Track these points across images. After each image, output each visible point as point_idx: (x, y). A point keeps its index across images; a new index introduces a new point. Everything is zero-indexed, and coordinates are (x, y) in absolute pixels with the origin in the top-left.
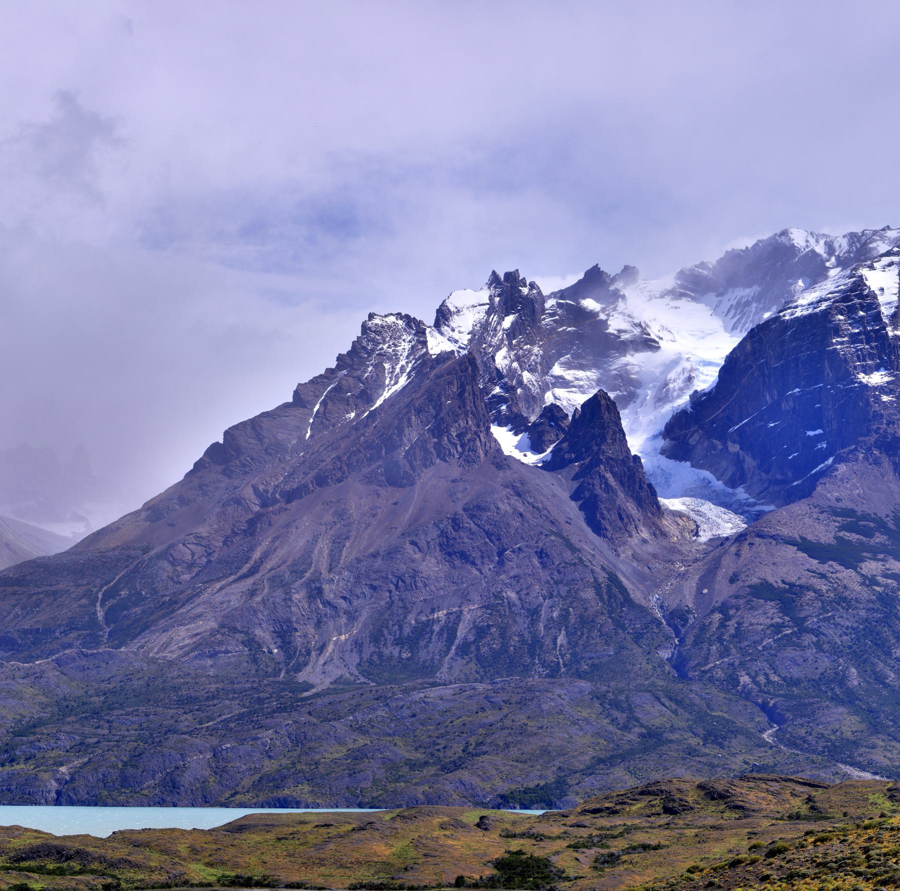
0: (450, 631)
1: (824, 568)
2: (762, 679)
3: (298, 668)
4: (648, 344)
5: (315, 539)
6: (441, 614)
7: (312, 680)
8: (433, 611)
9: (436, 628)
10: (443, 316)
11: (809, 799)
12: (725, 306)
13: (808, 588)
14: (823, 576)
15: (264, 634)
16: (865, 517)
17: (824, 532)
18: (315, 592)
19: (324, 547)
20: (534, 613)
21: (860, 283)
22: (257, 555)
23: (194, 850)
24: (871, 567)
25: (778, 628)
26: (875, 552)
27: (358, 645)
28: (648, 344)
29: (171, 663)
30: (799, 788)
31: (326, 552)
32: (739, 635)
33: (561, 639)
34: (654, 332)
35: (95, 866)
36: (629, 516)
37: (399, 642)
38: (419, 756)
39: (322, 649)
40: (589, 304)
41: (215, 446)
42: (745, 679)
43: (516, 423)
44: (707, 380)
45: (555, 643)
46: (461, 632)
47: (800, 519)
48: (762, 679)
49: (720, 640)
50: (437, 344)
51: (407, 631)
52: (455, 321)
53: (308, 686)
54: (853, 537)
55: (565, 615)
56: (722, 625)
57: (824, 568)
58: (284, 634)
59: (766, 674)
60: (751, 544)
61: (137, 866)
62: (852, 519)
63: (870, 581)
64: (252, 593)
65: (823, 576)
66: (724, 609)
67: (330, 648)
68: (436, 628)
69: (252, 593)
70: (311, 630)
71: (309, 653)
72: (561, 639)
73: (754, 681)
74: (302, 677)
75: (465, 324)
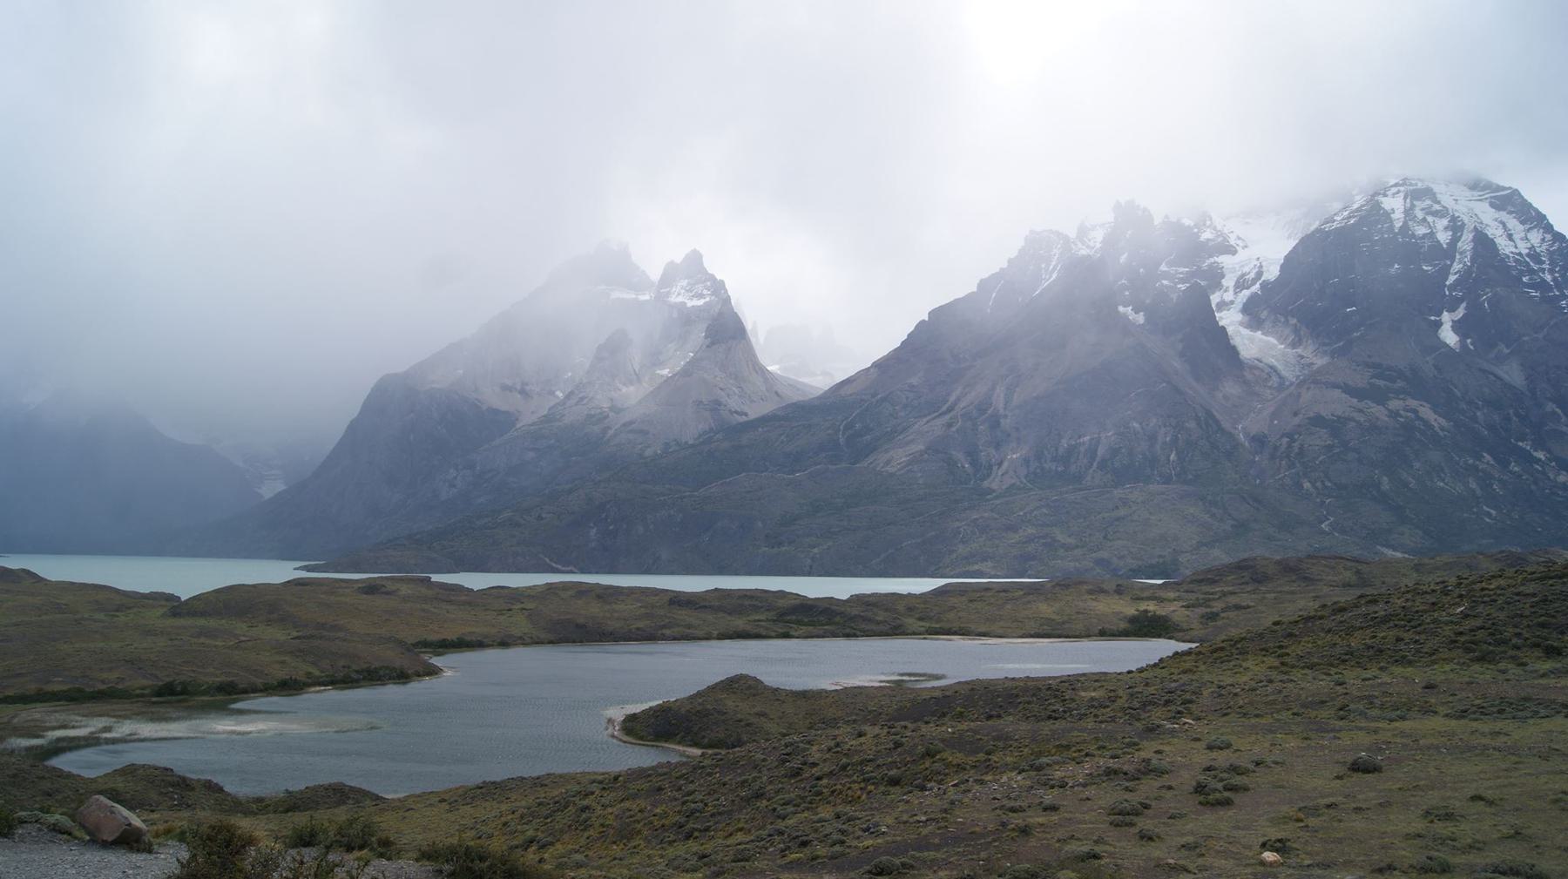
0: (1092, 453)
1: (1361, 405)
3: (983, 480)
7: (994, 486)
9: (1082, 449)
11: (1358, 572)
13: (1352, 419)
14: (1361, 411)
15: (959, 456)
18: (995, 423)
20: (1152, 438)
21: (1378, 205)
22: (952, 399)
23: (910, 609)
24: (1395, 404)
25: (1330, 448)
27: (1026, 461)
29: (892, 475)
30: (1349, 564)
33: (1172, 457)
35: (838, 619)
37: (1054, 459)
38: (1071, 541)
39: (1000, 464)
41: (922, 322)
42: (1307, 485)
46: (1101, 452)
49: (1288, 457)
51: (1061, 451)
54: (1381, 383)
55: (1175, 440)
56: (1289, 446)
57: (1361, 405)
58: (972, 454)
61: (870, 620)
63: (1394, 414)
64: (950, 425)
65: (1361, 411)
66: (1290, 435)
67: (1006, 464)
68: (1082, 449)
69: (950, 425)
70: (992, 451)
71: (990, 467)
72: (1172, 457)
73: (1313, 485)
74: (986, 484)
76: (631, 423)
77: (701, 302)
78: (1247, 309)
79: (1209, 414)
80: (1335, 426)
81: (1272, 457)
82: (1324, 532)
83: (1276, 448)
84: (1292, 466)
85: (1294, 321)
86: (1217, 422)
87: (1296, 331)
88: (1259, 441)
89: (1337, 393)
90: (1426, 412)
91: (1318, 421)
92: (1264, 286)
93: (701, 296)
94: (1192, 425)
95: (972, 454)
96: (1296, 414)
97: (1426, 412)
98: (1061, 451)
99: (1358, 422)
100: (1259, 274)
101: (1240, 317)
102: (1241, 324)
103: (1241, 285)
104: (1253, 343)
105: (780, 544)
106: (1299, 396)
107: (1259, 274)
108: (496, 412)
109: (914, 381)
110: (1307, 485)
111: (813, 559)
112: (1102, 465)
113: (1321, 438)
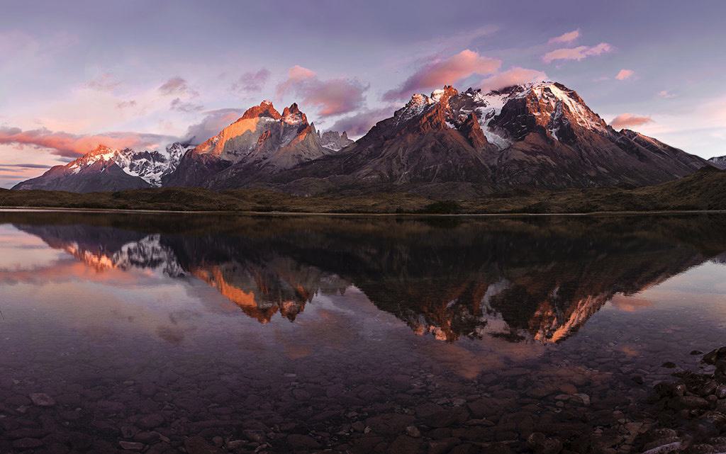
0: (434, 171)
4: (485, 105)
6: (432, 167)
16: (537, 145)
17: (528, 148)
24: (539, 157)
26: (540, 153)
28: (485, 105)
33: (464, 173)
34: (485, 102)
39: (400, 176)
40: (469, 95)
42: (511, 183)
44: (498, 113)
47: (521, 145)
50: (431, 101)
62: (534, 146)
63: (539, 160)
71: (396, 177)
75: (438, 98)
78: (489, 125)
87: (506, 133)
89: (520, 152)
90: (549, 160)
97: (549, 160)
99: (528, 163)
100: (494, 113)
103: (488, 117)
104: (491, 137)
107: (494, 113)
108: (225, 161)
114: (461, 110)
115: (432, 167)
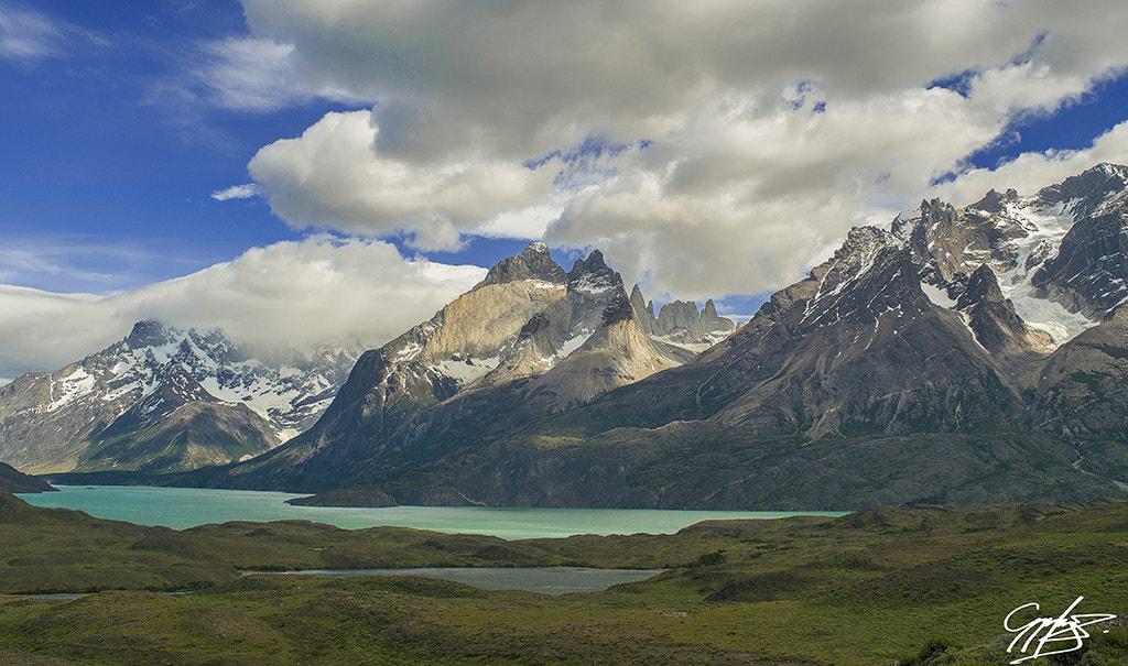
0: (894, 406)
2: (1076, 429)
5: (817, 356)
6: (889, 396)
7: (813, 436)
8: (884, 394)
9: (885, 404)
10: (896, 226)
12: (1069, 208)
14: (1117, 367)
15: (787, 411)
18: (817, 385)
19: (822, 359)
27: (840, 414)
31: (824, 361)
32: (1064, 404)
36: (1003, 334)
39: (820, 418)
42: (1066, 430)
43: (939, 281)
44: (1054, 253)
45: (954, 411)
48: (1076, 429)
52: (904, 228)
53: (809, 439)
56: (1054, 398)
59: (1079, 427)
60: (1073, 350)
64: (780, 387)
67: (824, 417)
68: (885, 404)
73: (1072, 431)
76: (543, 387)
77: (601, 290)
79: (991, 372)
80: (1092, 380)
81: (1039, 408)
82: (1072, 469)
83: (1043, 400)
84: (1055, 414)
85: (1072, 291)
86: (997, 379)
87: (1075, 299)
88: (1029, 394)
91: (1080, 377)
92: (1047, 263)
93: (600, 285)
94: (976, 382)
95: (798, 410)
96: (1061, 371)
98: (869, 405)
101: (1030, 289)
102: (1031, 295)
103: (1030, 263)
105: (637, 484)
106: (1066, 356)
109: (756, 351)
110: (1066, 430)
111: (660, 496)
112: (901, 417)
113: (1081, 391)
114: (967, 251)
115: (889, 396)
